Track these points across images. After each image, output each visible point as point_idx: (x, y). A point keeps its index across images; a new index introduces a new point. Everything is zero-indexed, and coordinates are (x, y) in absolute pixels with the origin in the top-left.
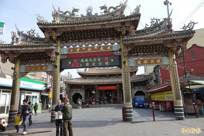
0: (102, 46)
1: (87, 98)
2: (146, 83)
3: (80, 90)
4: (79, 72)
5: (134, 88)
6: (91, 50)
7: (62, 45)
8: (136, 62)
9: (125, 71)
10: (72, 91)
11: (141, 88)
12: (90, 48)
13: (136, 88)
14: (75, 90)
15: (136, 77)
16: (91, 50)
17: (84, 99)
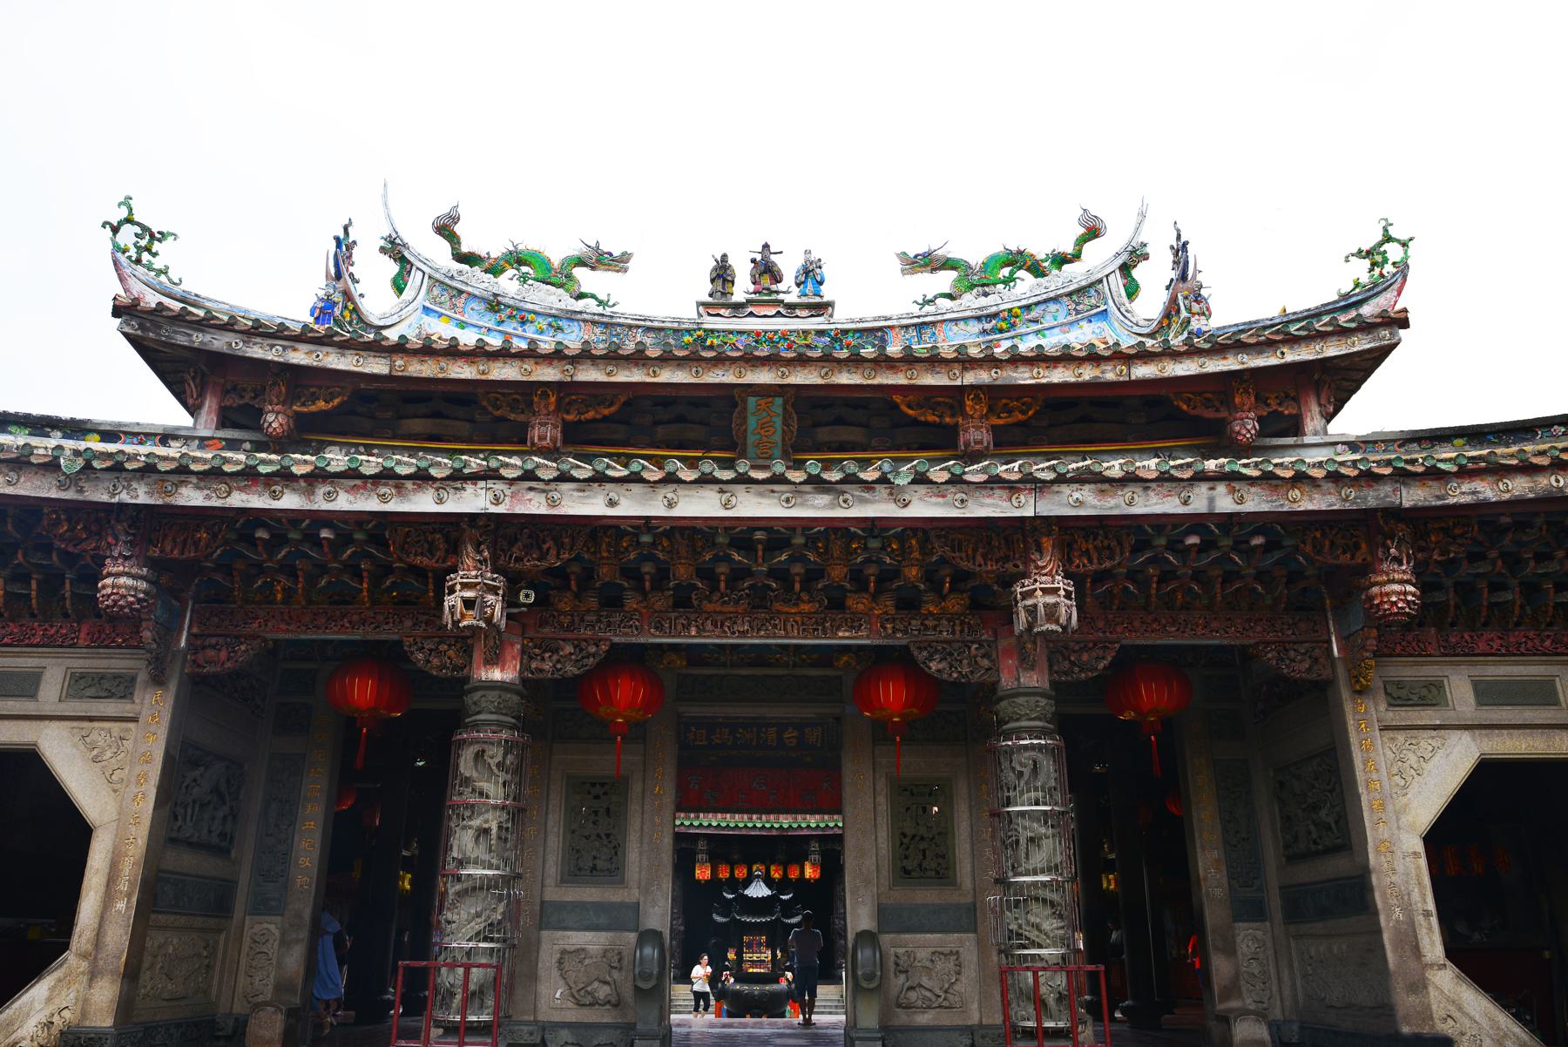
3: (80, 685)
4: (151, 299)
5: (1399, 697)
13: (1431, 695)
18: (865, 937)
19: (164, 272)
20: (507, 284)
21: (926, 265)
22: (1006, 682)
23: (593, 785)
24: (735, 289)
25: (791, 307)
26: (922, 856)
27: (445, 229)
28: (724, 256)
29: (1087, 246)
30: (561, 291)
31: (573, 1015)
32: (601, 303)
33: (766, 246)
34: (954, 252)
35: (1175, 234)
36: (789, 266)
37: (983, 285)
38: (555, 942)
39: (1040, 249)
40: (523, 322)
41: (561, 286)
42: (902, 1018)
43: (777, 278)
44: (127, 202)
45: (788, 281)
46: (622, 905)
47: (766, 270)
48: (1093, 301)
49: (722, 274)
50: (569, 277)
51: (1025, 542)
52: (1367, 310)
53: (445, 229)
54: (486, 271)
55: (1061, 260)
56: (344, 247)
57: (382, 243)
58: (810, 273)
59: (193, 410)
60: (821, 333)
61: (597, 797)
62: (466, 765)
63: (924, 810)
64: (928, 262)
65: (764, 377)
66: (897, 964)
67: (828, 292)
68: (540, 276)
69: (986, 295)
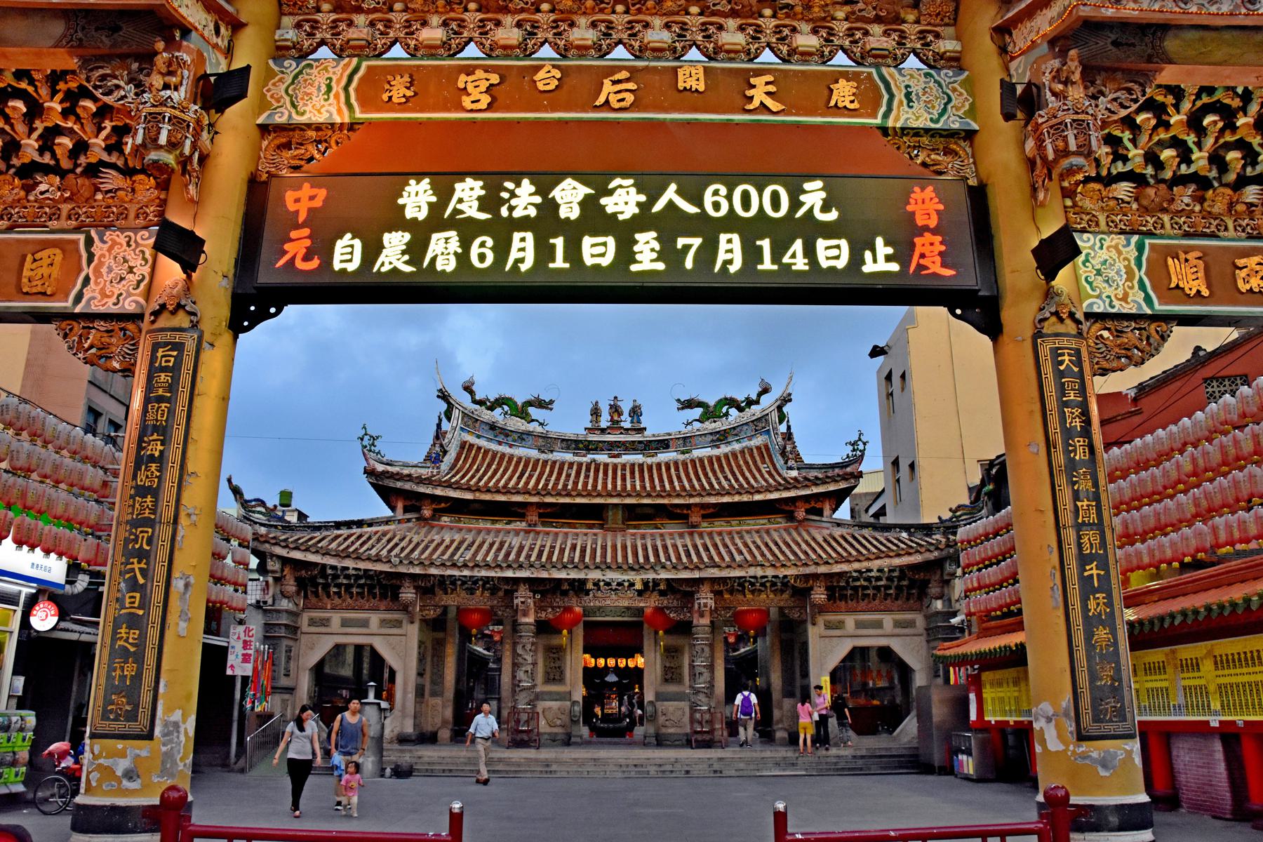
0: (759, 73)
1: (434, 694)
2: (924, 585)
6: (630, 98)
7: (289, 34)
8: (1158, 272)
9: (1056, 353)
10: (312, 622)
11: (878, 624)
12: (624, 75)
14: (336, 618)
15: (843, 537)
16: (630, 98)
17: (411, 696)
18: (651, 702)
19: (379, 453)
20: (497, 415)
22: (695, 622)
25: (627, 430)
26: (671, 675)
27: (468, 389)
29: (762, 397)
31: (549, 730)
32: (541, 424)
34: (702, 398)
36: (626, 408)
38: (541, 706)
39: (740, 397)
40: (507, 435)
42: (664, 730)
44: (364, 427)
45: (625, 416)
46: (565, 693)
47: (615, 409)
49: (596, 412)
50: (527, 414)
52: (849, 470)
53: (468, 389)
55: (750, 402)
58: (636, 412)
59: (393, 509)
60: (640, 442)
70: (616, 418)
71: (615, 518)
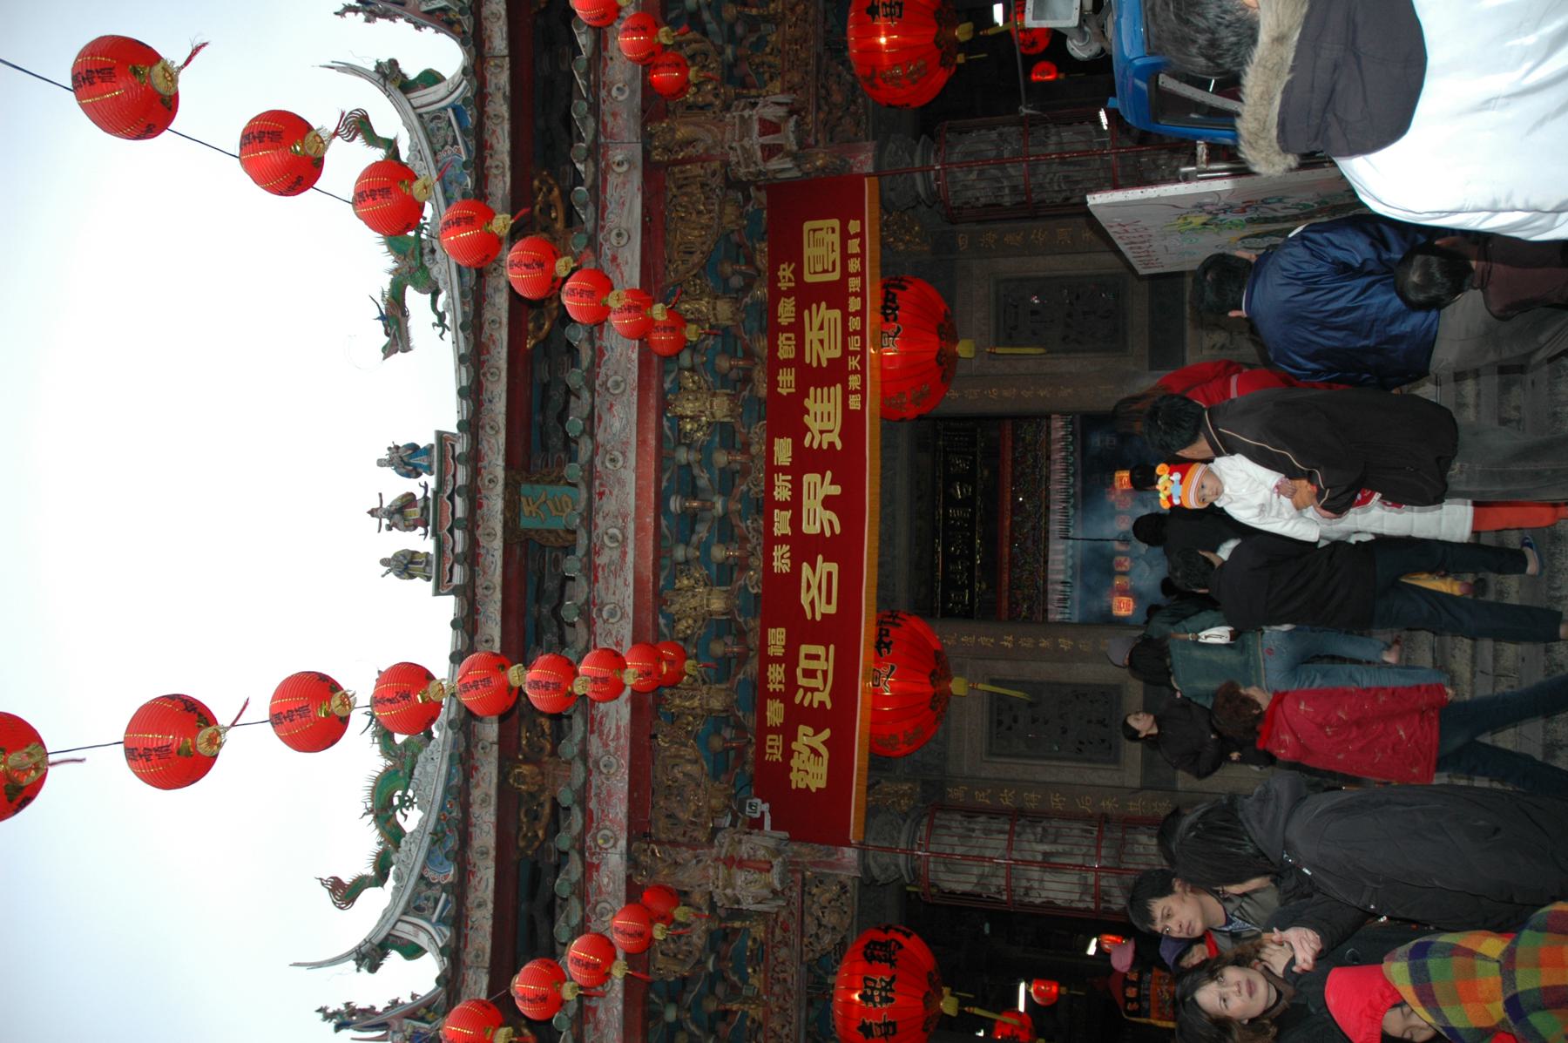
20: (411, 820)
21: (398, 323)
23: (1000, 723)
24: (422, 550)
28: (384, 562)
30: (421, 758)
33: (372, 513)
35: (350, 15)
36: (396, 486)
37: (422, 255)
41: (415, 756)
43: (409, 499)
47: (400, 514)
48: (444, 125)
49: (405, 565)
51: (684, 162)
54: (397, 846)
56: (346, 1018)
57: (364, 970)
58: (406, 460)
61: (1015, 720)
62: (962, 882)
63: (1034, 312)
64: (394, 318)
65: (495, 504)
66: (1222, 347)
67: (426, 439)
68: (404, 783)
69: (433, 251)
70: (414, 513)
71: (547, 508)
